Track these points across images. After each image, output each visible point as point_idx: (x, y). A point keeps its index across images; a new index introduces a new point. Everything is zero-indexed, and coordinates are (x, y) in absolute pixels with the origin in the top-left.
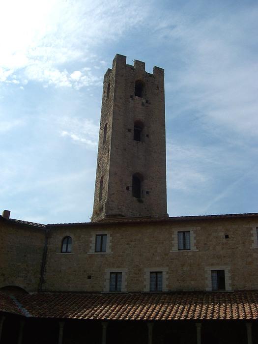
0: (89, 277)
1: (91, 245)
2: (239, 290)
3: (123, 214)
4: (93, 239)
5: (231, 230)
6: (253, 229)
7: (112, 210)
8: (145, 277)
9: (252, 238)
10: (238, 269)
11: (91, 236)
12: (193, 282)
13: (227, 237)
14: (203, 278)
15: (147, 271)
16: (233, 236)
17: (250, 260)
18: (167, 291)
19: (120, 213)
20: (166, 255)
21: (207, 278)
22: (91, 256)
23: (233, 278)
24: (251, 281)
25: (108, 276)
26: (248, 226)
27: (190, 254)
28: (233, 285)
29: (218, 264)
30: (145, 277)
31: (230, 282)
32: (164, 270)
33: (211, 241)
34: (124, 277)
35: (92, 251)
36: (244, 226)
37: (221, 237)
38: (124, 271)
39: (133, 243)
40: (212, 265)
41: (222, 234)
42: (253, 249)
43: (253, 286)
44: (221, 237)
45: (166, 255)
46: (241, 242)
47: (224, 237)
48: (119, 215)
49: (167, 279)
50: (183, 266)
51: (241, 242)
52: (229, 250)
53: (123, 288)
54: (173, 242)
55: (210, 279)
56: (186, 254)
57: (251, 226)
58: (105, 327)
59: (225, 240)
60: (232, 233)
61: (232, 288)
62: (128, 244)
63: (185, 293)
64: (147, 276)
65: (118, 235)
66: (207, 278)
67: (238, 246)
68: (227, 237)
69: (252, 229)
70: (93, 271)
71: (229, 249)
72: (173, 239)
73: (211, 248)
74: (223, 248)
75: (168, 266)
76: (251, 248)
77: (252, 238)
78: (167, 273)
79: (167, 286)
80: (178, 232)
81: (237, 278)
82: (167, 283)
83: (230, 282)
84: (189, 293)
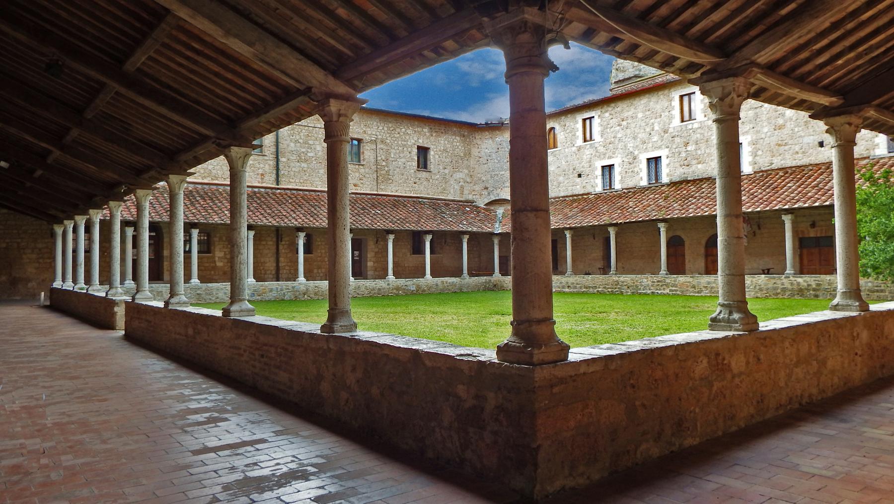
0: (580, 176)
1: (578, 134)
3: (641, 73)
4: (580, 125)
7: (624, 71)
8: (641, 166)
11: (577, 122)
12: (700, 166)
15: (643, 157)
17: (781, 121)
19: (637, 73)
20: (666, 132)
22: (579, 148)
23: (754, 155)
25: (599, 172)
27: (696, 126)
30: (641, 166)
31: (750, 159)
32: (663, 153)
34: (617, 170)
35: (580, 142)
38: (616, 161)
39: (624, 123)
45: (666, 132)
48: (636, 76)
49: (668, 165)
50: (686, 144)
53: (617, 186)
54: (673, 112)
56: (690, 127)
58: (568, 236)
62: (619, 125)
63: (688, 182)
64: (644, 165)
65: (607, 115)
70: (583, 167)
71: (750, 109)
72: (673, 108)
75: (667, 147)
80: (682, 97)
81: (760, 153)
82: (667, 171)
84: (694, 181)
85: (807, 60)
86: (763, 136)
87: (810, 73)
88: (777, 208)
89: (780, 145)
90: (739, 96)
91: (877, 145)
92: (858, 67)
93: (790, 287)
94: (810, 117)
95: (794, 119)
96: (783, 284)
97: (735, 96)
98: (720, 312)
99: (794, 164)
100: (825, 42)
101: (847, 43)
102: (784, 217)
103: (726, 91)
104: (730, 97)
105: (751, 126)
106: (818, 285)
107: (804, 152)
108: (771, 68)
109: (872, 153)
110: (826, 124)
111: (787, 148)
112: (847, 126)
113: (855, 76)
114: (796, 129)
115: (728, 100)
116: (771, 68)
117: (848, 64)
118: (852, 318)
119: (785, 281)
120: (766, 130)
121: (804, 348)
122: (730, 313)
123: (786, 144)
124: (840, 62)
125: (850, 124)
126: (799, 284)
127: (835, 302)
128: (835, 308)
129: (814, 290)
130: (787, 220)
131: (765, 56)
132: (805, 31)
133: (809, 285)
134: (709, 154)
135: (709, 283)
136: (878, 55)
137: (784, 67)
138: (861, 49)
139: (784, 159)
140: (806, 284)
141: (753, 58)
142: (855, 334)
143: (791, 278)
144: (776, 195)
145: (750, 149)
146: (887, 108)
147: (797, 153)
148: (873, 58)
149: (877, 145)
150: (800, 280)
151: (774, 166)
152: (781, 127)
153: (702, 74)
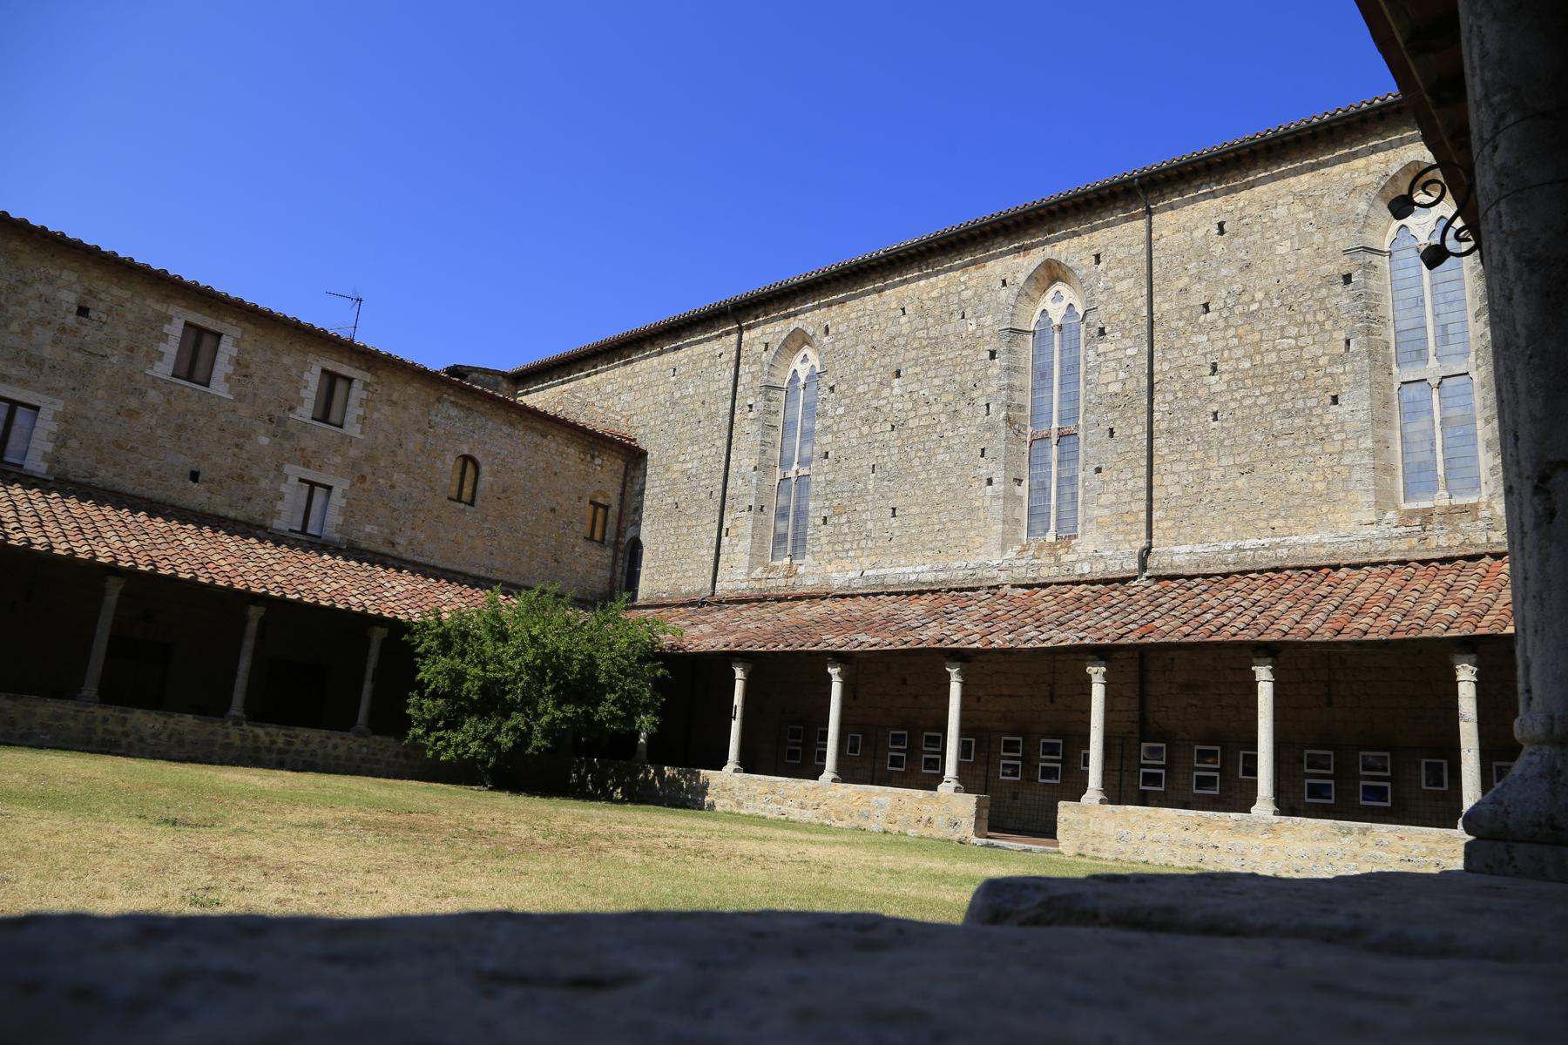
5: (103, 296)
6: (175, 320)
9: (162, 347)
13: (83, 311)
16: (104, 318)
17: (133, 403)
23: (61, 440)
24: (115, 464)
26: (158, 307)
28: (54, 460)
29: (23, 383)
31: (49, 447)
33: (21, 304)
36: (148, 302)
37: (65, 306)
41: (69, 298)
42: (154, 379)
43: (116, 479)
44: (65, 306)
46: (123, 344)
47: (75, 309)
51: (123, 344)
52: (77, 355)
57: (170, 312)
59: (71, 319)
60: (102, 306)
61: (51, 468)
67: (109, 351)
68: (83, 311)
69: (170, 319)
73: (14, 327)
74: (55, 342)
76: (148, 372)
77: (162, 347)
81: (74, 443)
83: (49, 447)
86: (92, 415)
89: (119, 446)
91: (279, 513)
93: (238, 742)
95: (161, 411)
96: (227, 736)
99: (138, 491)
105: (70, 384)
106: (289, 743)
107: (161, 478)
109: (268, 523)
111: (131, 456)
114: (159, 432)
119: (234, 733)
120: (100, 405)
123: (133, 450)
126: (256, 737)
129: (280, 751)
130: (255, 613)
133: (273, 742)
135: (58, 717)
139: (120, 475)
140: (267, 740)
143: (245, 726)
145: (54, 427)
147: (149, 474)
149: (279, 513)
150: (259, 731)
152: (132, 413)
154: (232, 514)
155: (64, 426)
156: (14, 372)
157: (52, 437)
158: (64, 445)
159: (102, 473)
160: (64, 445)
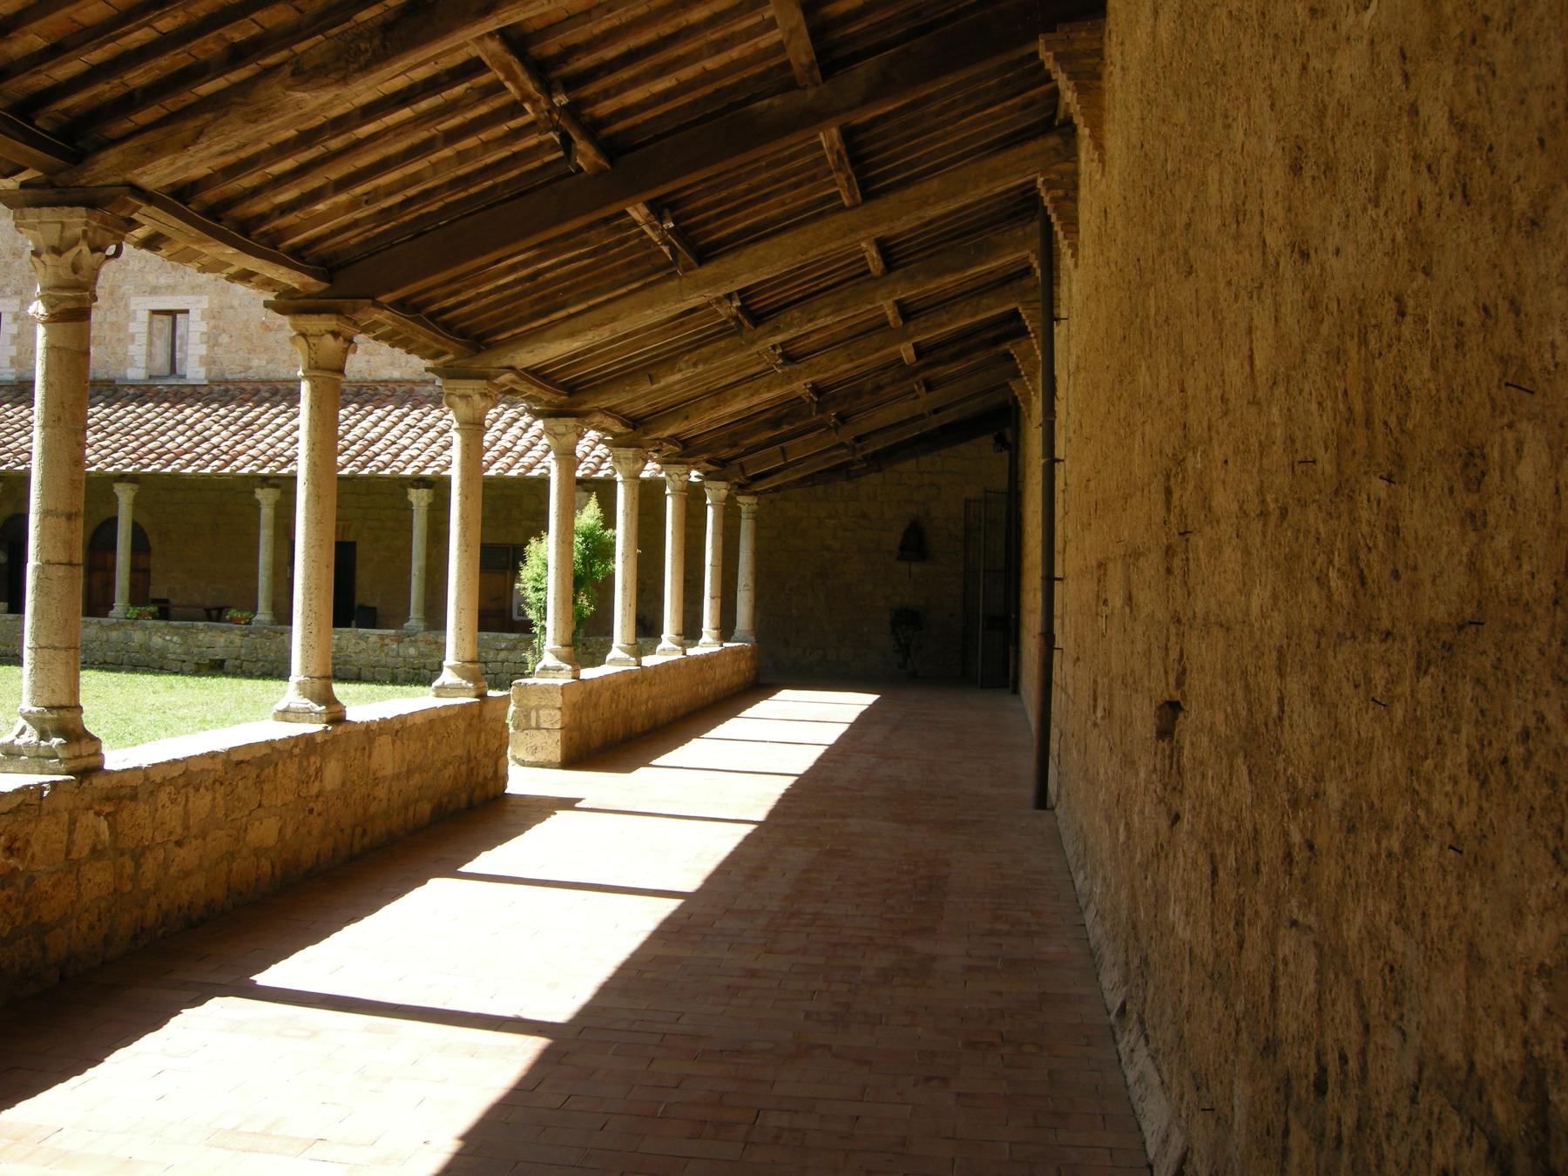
2: (230, 377)
10: (232, 307)
14: (122, 336)
18: (12, 377)
21: (132, 338)
23: (212, 340)
24: (266, 350)
28: (209, 361)
29: (172, 289)
31: (203, 350)
40: (154, 291)
55: (142, 339)
61: (209, 371)
66: (132, 338)
75: (18, 293)
78: (16, 318)
79: (12, 362)
81: (224, 339)
83: (203, 350)
85: (255, 192)
86: (235, 303)
87: (262, 218)
88: (245, 471)
90: (94, 250)
92: (355, 224)
94: (267, 304)
97: (85, 248)
98: (23, 731)
100: (288, 164)
101: (335, 173)
102: (260, 494)
103: (68, 234)
104: (75, 250)
108: (180, 198)
110: (294, 326)
112: (329, 339)
113: (353, 237)
115: (70, 255)
116: (180, 198)
117: (330, 217)
118: (308, 739)
121: (202, 803)
122: (43, 735)
124: (321, 207)
125: (336, 334)
127: (281, 706)
128: (285, 715)
131: (158, 174)
132: (232, 143)
134: (112, 324)
136: (390, 208)
137: (210, 196)
138: (359, 190)
141: (129, 176)
142: (312, 770)
144: (249, 442)
145: (203, 327)
146: (417, 309)
148: (383, 211)
151: (251, 374)
153: (24, 185)
154: (396, 375)
155: (213, 322)
156: (162, 281)
157: (205, 338)
158: (216, 344)
159: (255, 363)
160: (216, 344)
